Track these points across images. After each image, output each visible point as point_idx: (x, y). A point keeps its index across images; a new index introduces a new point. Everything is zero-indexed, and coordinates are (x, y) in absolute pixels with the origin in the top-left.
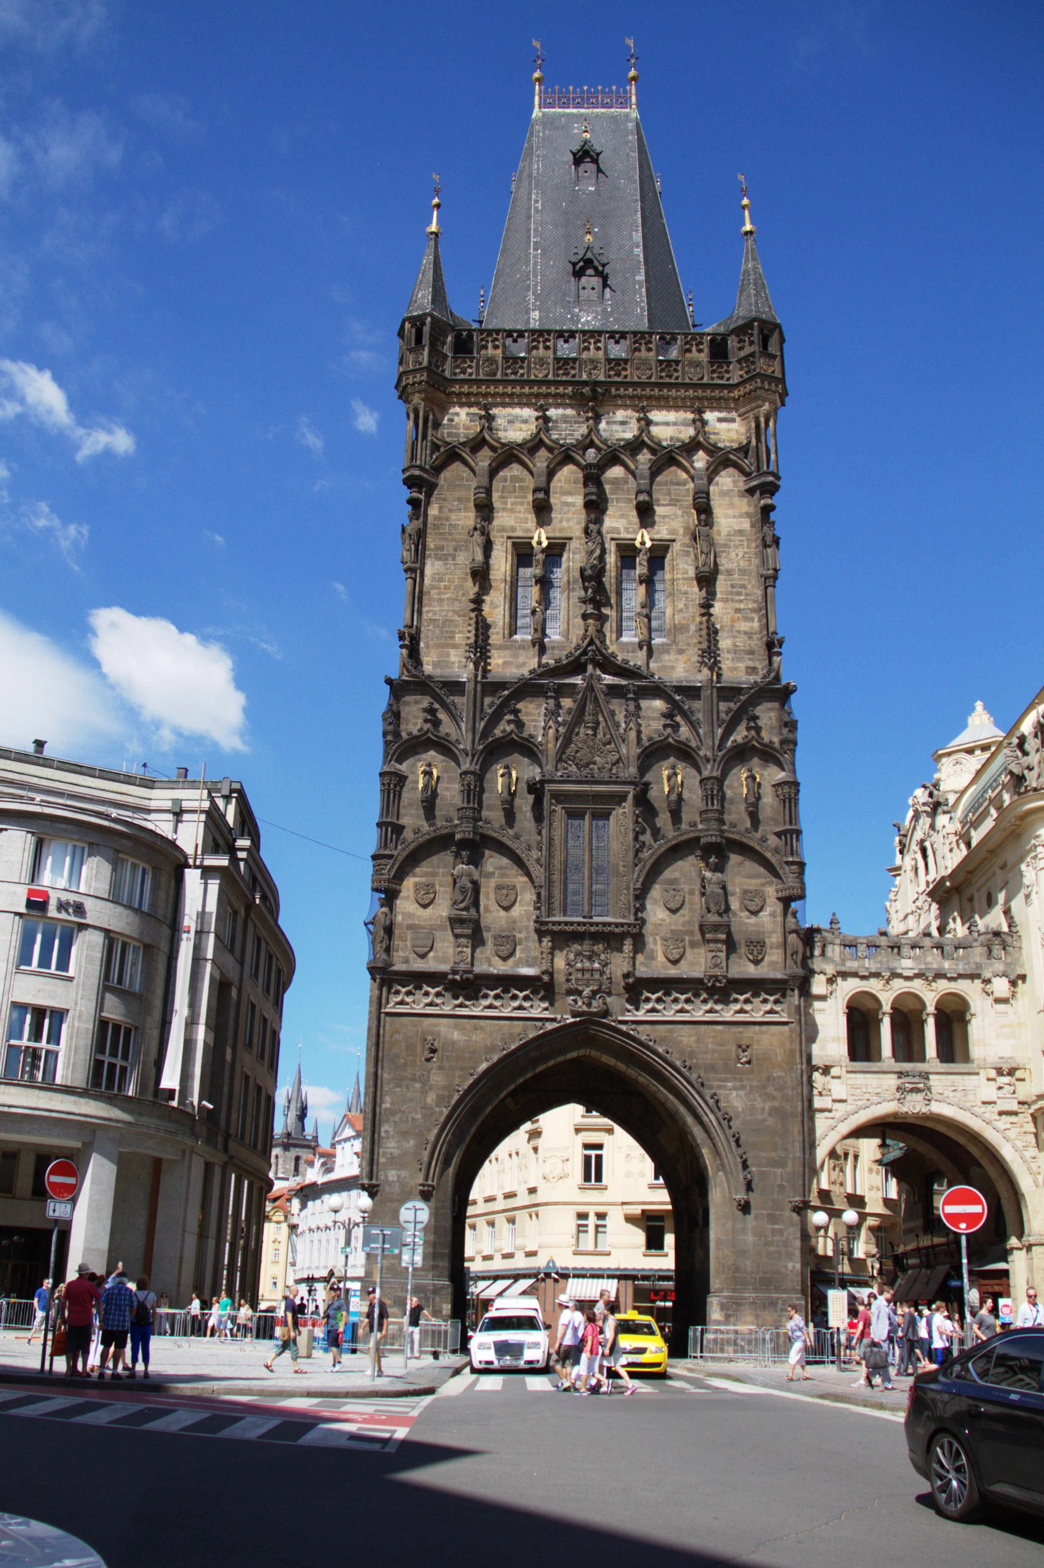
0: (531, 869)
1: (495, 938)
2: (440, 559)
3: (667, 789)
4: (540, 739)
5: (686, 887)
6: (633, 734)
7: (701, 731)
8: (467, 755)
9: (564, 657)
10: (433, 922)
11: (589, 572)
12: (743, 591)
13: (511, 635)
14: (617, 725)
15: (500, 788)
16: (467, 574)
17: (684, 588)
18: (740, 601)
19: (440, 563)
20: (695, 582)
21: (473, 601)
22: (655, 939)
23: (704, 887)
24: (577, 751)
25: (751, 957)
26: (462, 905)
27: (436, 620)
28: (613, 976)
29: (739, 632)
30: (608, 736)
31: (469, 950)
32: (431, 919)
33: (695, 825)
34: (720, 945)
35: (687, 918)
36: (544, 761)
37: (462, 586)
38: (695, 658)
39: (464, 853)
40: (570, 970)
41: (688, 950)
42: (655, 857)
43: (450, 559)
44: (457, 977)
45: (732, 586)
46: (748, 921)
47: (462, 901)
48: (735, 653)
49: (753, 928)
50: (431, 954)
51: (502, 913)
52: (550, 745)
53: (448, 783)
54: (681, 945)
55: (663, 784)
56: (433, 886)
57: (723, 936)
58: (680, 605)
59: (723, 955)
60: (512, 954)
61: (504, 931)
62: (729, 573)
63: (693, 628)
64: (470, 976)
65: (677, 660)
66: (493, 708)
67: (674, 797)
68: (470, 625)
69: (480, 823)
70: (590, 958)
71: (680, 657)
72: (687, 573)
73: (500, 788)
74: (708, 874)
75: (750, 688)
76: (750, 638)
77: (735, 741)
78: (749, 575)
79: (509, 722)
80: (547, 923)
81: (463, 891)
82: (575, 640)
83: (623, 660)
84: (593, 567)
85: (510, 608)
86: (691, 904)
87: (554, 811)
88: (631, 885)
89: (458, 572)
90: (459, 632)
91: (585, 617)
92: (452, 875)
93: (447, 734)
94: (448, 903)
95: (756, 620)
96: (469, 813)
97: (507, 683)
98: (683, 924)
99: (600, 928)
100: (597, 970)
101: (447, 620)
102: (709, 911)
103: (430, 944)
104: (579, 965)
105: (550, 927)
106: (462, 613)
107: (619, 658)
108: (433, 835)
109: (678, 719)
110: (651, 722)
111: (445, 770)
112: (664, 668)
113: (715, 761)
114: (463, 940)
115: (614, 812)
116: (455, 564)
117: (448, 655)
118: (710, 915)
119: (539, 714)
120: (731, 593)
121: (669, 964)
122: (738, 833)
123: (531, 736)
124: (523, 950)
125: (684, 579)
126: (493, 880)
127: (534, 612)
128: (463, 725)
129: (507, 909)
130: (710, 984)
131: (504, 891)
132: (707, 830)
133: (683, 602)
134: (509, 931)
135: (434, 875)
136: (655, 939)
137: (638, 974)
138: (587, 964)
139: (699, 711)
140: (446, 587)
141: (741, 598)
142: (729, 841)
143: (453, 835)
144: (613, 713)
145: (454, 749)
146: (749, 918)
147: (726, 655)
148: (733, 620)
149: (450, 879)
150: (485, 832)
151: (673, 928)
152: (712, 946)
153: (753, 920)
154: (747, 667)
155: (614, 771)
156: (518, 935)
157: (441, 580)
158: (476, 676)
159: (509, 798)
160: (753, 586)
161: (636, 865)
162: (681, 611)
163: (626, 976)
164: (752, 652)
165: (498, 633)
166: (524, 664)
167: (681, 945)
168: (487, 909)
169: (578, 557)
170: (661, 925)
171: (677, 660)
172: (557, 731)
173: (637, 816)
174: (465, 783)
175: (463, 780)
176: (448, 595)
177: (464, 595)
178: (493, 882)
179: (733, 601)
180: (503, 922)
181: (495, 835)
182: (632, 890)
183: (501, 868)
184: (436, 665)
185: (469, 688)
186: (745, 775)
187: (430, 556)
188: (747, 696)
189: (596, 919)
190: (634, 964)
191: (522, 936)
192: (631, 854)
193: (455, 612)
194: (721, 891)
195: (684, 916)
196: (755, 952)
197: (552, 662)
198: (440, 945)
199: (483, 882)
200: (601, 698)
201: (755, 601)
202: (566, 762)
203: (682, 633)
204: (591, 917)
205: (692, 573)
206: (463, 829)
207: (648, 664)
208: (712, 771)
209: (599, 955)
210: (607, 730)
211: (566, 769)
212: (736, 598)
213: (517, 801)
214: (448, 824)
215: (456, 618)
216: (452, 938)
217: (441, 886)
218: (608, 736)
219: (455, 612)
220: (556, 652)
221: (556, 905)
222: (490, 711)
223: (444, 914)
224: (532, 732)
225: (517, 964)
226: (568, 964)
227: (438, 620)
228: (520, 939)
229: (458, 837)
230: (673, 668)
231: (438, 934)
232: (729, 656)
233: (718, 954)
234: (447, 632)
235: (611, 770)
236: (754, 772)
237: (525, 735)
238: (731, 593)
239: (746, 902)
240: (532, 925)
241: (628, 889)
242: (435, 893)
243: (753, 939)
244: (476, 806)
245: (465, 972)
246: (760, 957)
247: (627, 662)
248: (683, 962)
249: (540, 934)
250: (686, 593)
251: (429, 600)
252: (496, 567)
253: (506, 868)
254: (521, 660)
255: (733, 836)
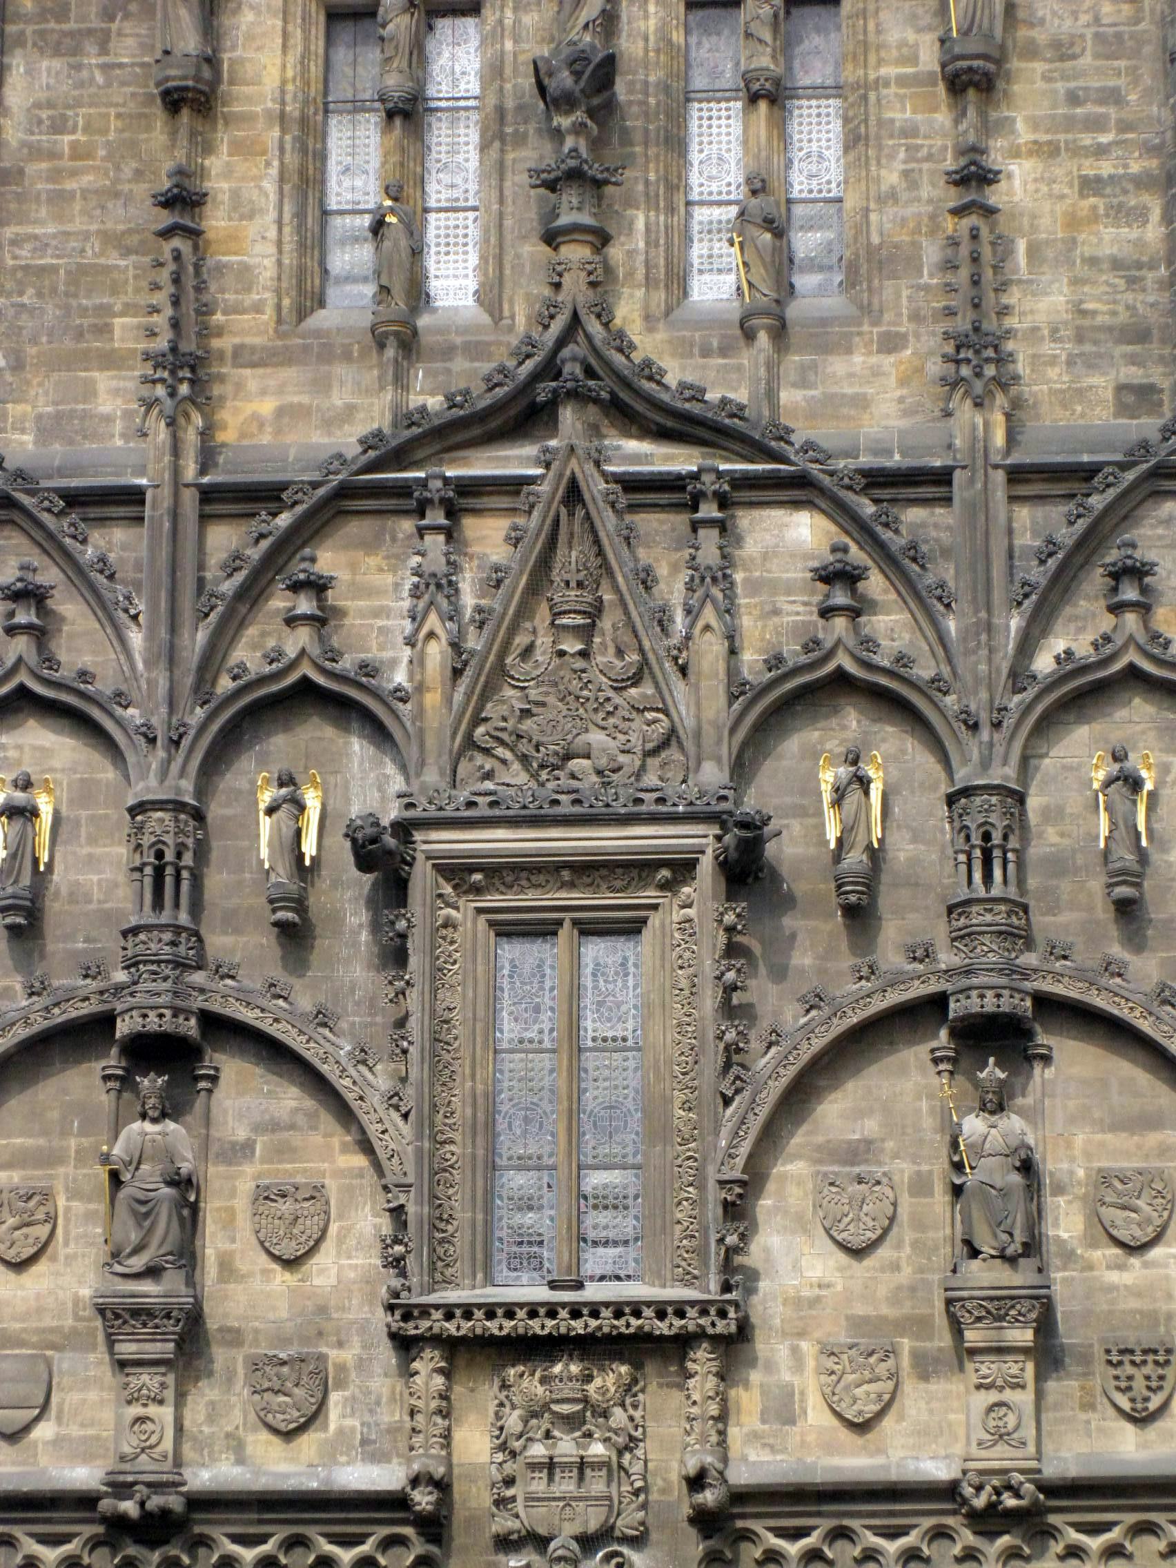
0: (373, 1130)
1: (255, 1366)
2: (57, 52)
3: (832, 833)
4: (400, 677)
5: (903, 1169)
6: (710, 650)
7: (951, 625)
8: (152, 741)
9: (478, 388)
10: (48, 1322)
11: (564, 80)
12: (1112, 112)
13: (302, 314)
14: (663, 622)
15: (264, 853)
16: (149, 99)
17: (901, 114)
18: (1101, 151)
19: (57, 64)
20: (941, 89)
21: (169, 202)
22: (795, 1350)
23: (958, 1167)
24: (526, 713)
25: (1126, 1405)
26: (138, 1263)
27: (43, 269)
28: (657, 1483)
29: (1093, 261)
30: (634, 657)
31: (165, 1413)
32: (40, 1311)
33: (928, 954)
34: (1011, 1366)
35: (906, 1275)
36: (412, 753)
37: (133, 144)
38: (935, 367)
39: (145, 1082)
40: (509, 1468)
41: (909, 1386)
42: (790, 1073)
43: (91, 48)
44: (129, 1507)
45: (1074, 99)
46: (1114, 1277)
47: (136, 1251)
48: (1080, 338)
49: (1133, 1304)
50: (44, 1431)
51: (282, 1279)
52: (432, 699)
53: (92, 840)
54: (882, 1370)
55: (819, 813)
56: (47, 1196)
57: (1024, 1336)
58: (891, 177)
59: (1024, 1398)
60: (313, 1419)
61: (285, 1341)
62: (1063, 50)
63: (931, 253)
64: (174, 1502)
65: (876, 372)
66: (239, 577)
67: (855, 858)
68: (155, 287)
69: (198, 978)
70: (572, 1422)
71: (887, 361)
72: (913, 60)
73: (264, 853)
74: (973, 1125)
75: (1124, 466)
76: (1131, 281)
77: (1069, 653)
78: (1136, 53)
79: (291, 621)
80: (425, 1311)
81: (143, 1211)
82: (521, 322)
83: (683, 386)
84: (577, 61)
85: (301, 215)
86: (919, 1224)
87: (448, 924)
88: (711, 1170)
89: (120, 94)
90: (128, 310)
91: (552, 238)
92: (106, 1159)
93: (84, 675)
94: (98, 1253)
95: (1156, 214)
96: (158, 945)
97: (283, 486)
98: (895, 1298)
99: (606, 1323)
100: (604, 1464)
101: (82, 270)
102: (974, 1253)
103: (41, 1400)
104: (538, 1451)
105: (436, 1323)
106: (134, 240)
107: (671, 380)
108: (40, 1024)
109: (875, 584)
110: (782, 601)
111: (85, 793)
112: (832, 405)
113: (997, 725)
114: (147, 1379)
115: (655, 920)
116: (106, 68)
117: (89, 392)
118: (975, 1264)
119: (397, 586)
120: (1070, 123)
121: (844, 1434)
122: (1080, 975)
123: (369, 669)
124: (352, 1405)
125: (902, 81)
126: (249, 1169)
127: (378, 227)
128: (136, 638)
129: (290, 1264)
130: (980, 1502)
131: (285, 1207)
132: (968, 972)
133: (899, 166)
134: (305, 1340)
135: (50, 1159)
136: (795, 1350)
137: (740, 1476)
138: (566, 1447)
139: (946, 553)
140: (78, 153)
141: (1104, 139)
142: (1046, 1005)
143: (107, 1021)
144: (646, 580)
145: (109, 725)
146: (1121, 1267)
147: (1048, 348)
148: (1073, 222)
149: (102, 1174)
150: (216, 1006)
151: (860, 1310)
152: (988, 1367)
153: (1134, 1272)
154: (1121, 388)
155: (651, 779)
156: (334, 1354)
157: (59, 126)
158: (176, 472)
159: (293, 887)
160: (1147, 94)
161: (727, 1101)
162: (892, 196)
163: (696, 1482)
164: (1137, 334)
165: (258, 308)
166: (351, 409)
167: (882, 1370)
168: (227, 1268)
169: (530, 19)
170: (815, 1302)
171: (876, 372)
172: (456, 646)
173: (730, 930)
174: (147, 840)
175: (140, 829)
176: (87, 180)
177: (139, 174)
178: (247, 1176)
179: (1076, 151)
180: (283, 1312)
181: (248, 1016)
182: (711, 1185)
183: (274, 1126)
184: (47, 429)
185: (157, 506)
186: (1100, 775)
187: (20, 41)
188: (1111, 493)
189: (593, 1292)
190: (722, 1443)
191: (347, 1355)
192: (713, 1059)
193: (109, 239)
194: (1016, 1178)
195: (896, 1267)
196: (1139, 1384)
197: (435, 402)
198: (74, 1397)
199: (214, 1175)
200: (608, 522)
201: (1150, 150)
202: (487, 751)
203: (894, 276)
204: (579, 1286)
205: (929, 58)
206: (139, 999)
207: (771, 395)
208: (985, 764)
209: (605, 1414)
210: (627, 638)
211: (488, 776)
212: (1087, 140)
213: (321, 899)
214: (93, 985)
215: (114, 259)
216: (106, 1372)
217: (73, 1194)
218: (634, 657)
219: (109, 239)
220: (460, 364)
221: (460, 1245)
222: (228, 587)
223: (86, 1292)
224: (373, 653)
225: (330, 1455)
226: (503, 1447)
227: (54, 269)
228: (342, 1368)
229: (123, 1028)
230: (862, 402)
231: (64, 1362)
232: (1060, 350)
233: (1009, 1395)
234: (84, 311)
235: (638, 775)
236: (1134, 761)
237: (347, 664)
238: (1070, 123)
239: (1108, 1213)
240: (380, 1320)
241: (699, 1182)
242: (52, 1219)
243: (1130, 1339)
244: (184, 918)
245: (155, 1487)
246: (1153, 1405)
247: (697, 394)
248: (888, 1423)
249: (405, 1345)
250: (910, 131)
251: (21, 198)
252: (249, 70)
253: (292, 1127)
254: (338, 399)
255: (1059, 989)
